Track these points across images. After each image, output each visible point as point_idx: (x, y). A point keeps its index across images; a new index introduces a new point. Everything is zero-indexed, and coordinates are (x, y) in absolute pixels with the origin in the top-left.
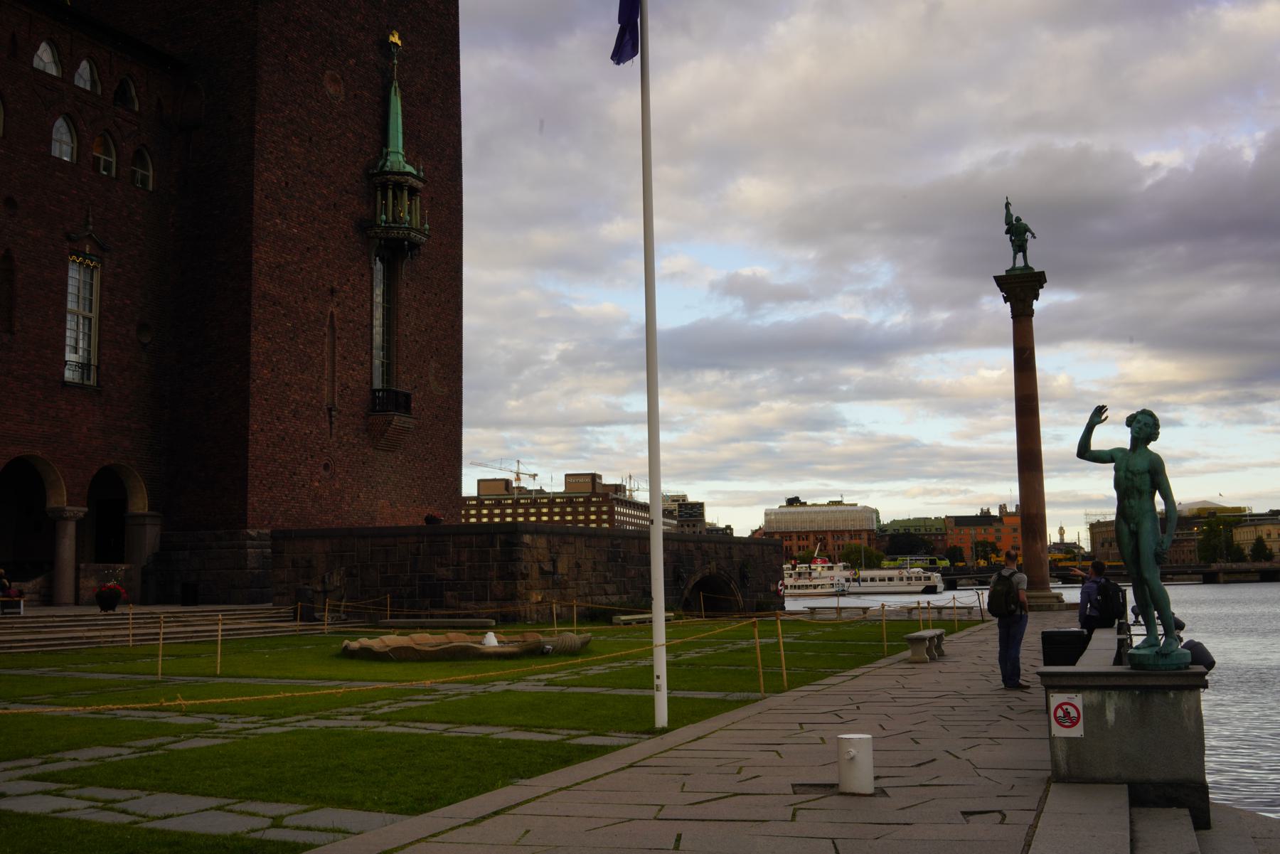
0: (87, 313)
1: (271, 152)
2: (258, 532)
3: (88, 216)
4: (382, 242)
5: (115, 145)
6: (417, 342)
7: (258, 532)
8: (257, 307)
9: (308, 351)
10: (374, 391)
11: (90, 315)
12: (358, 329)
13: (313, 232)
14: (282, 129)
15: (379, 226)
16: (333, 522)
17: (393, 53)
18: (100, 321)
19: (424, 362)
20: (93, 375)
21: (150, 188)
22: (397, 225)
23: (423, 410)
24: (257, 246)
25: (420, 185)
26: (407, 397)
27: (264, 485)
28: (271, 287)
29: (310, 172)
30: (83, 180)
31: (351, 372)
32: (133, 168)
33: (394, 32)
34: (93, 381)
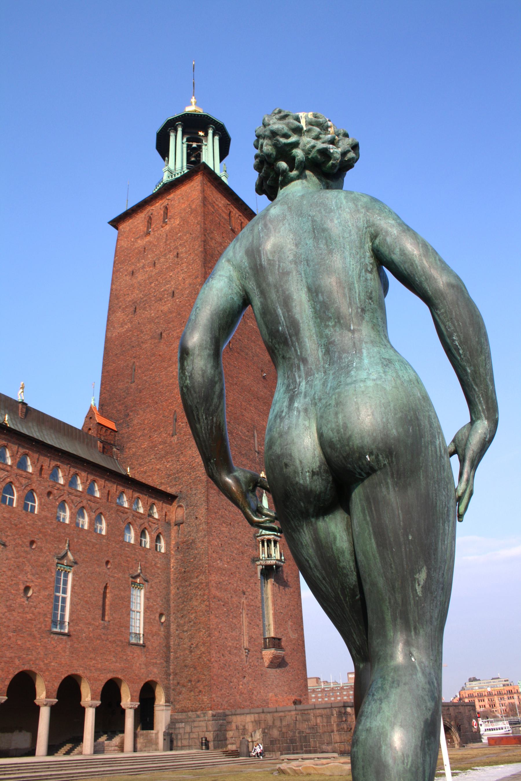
0: (138, 609)
15: (262, 560)
18: (144, 613)
20: (142, 639)
34: (141, 642)
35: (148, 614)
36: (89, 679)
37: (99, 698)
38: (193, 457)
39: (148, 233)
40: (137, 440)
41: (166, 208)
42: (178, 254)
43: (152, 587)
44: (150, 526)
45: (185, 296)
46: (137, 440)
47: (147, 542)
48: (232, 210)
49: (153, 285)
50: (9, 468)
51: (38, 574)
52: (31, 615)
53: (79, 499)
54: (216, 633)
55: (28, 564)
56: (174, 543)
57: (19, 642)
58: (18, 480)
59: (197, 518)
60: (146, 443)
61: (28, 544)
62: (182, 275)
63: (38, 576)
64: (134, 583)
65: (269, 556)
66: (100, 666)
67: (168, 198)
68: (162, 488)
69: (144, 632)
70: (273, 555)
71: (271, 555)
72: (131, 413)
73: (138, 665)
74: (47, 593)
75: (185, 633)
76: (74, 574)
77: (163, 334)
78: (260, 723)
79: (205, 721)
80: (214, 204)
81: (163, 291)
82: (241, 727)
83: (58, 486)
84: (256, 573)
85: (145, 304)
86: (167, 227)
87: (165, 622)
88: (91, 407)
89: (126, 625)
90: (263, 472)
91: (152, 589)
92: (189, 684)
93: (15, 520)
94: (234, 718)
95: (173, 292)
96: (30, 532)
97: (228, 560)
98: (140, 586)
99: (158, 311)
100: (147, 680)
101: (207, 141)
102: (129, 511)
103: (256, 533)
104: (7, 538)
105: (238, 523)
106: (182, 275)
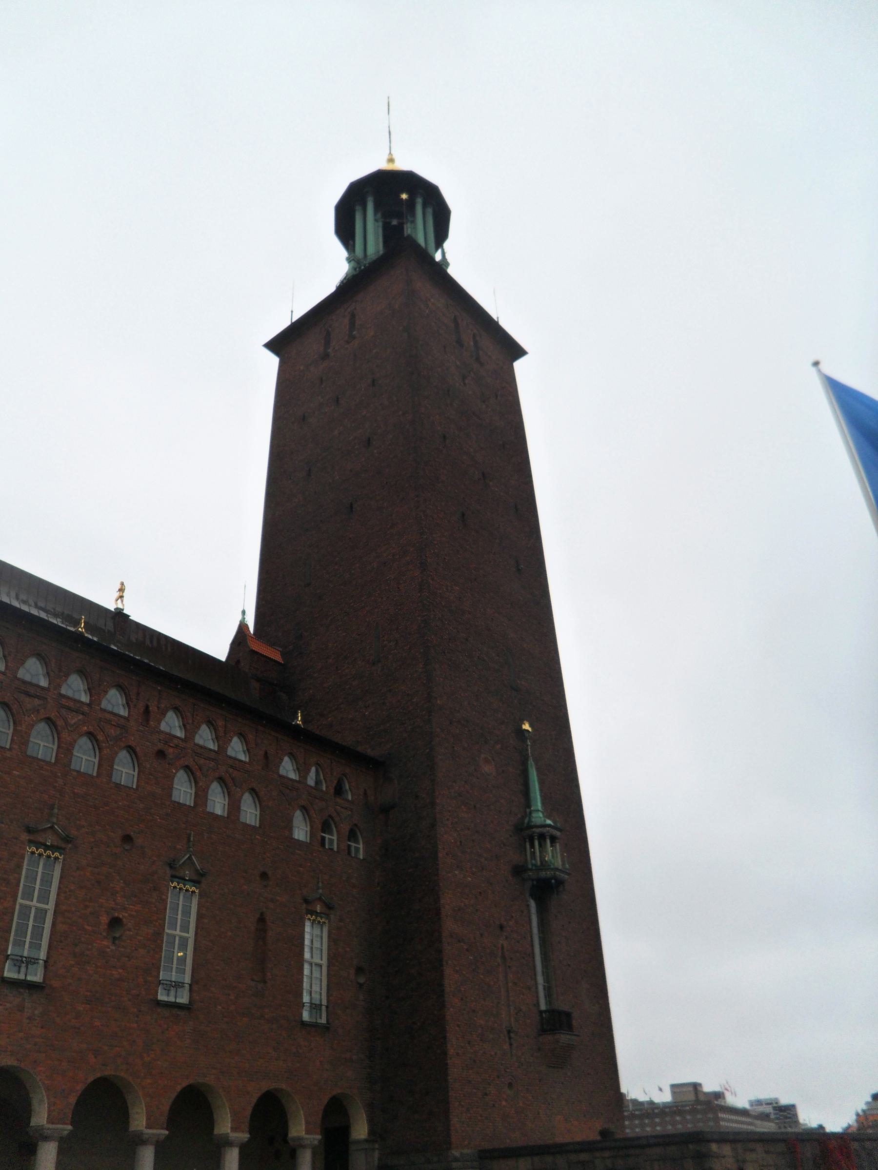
2: (461, 1153)
3: (318, 883)
4: (535, 883)
5: (336, 827)
6: (569, 965)
7: (461, 1153)
8: (447, 945)
10: (541, 1012)
12: (524, 958)
13: (483, 879)
15: (531, 870)
18: (328, 967)
21: (361, 857)
24: (443, 894)
25: (558, 834)
26: (568, 1015)
27: (463, 1106)
28: (456, 926)
30: (314, 854)
31: (522, 996)
32: (349, 843)
33: (525, 722)
34: (323, 1021)
39: (325, 356)
40: (315, 675)
41: (353, 316)
42: (373, 381)
44: (338, 814)
46: (315, 675)
47: (333, 839)
49: (336, 432)
50: (86, 708)
51: (135, 896)
52: (120, 971)
57: (97, 1023)
68: (360, 749)
69: (328, 1001)
83: (176, 741)
91: (342, 924)
95: (369, 439)
100: (334, 1093)
101: (413, 222)
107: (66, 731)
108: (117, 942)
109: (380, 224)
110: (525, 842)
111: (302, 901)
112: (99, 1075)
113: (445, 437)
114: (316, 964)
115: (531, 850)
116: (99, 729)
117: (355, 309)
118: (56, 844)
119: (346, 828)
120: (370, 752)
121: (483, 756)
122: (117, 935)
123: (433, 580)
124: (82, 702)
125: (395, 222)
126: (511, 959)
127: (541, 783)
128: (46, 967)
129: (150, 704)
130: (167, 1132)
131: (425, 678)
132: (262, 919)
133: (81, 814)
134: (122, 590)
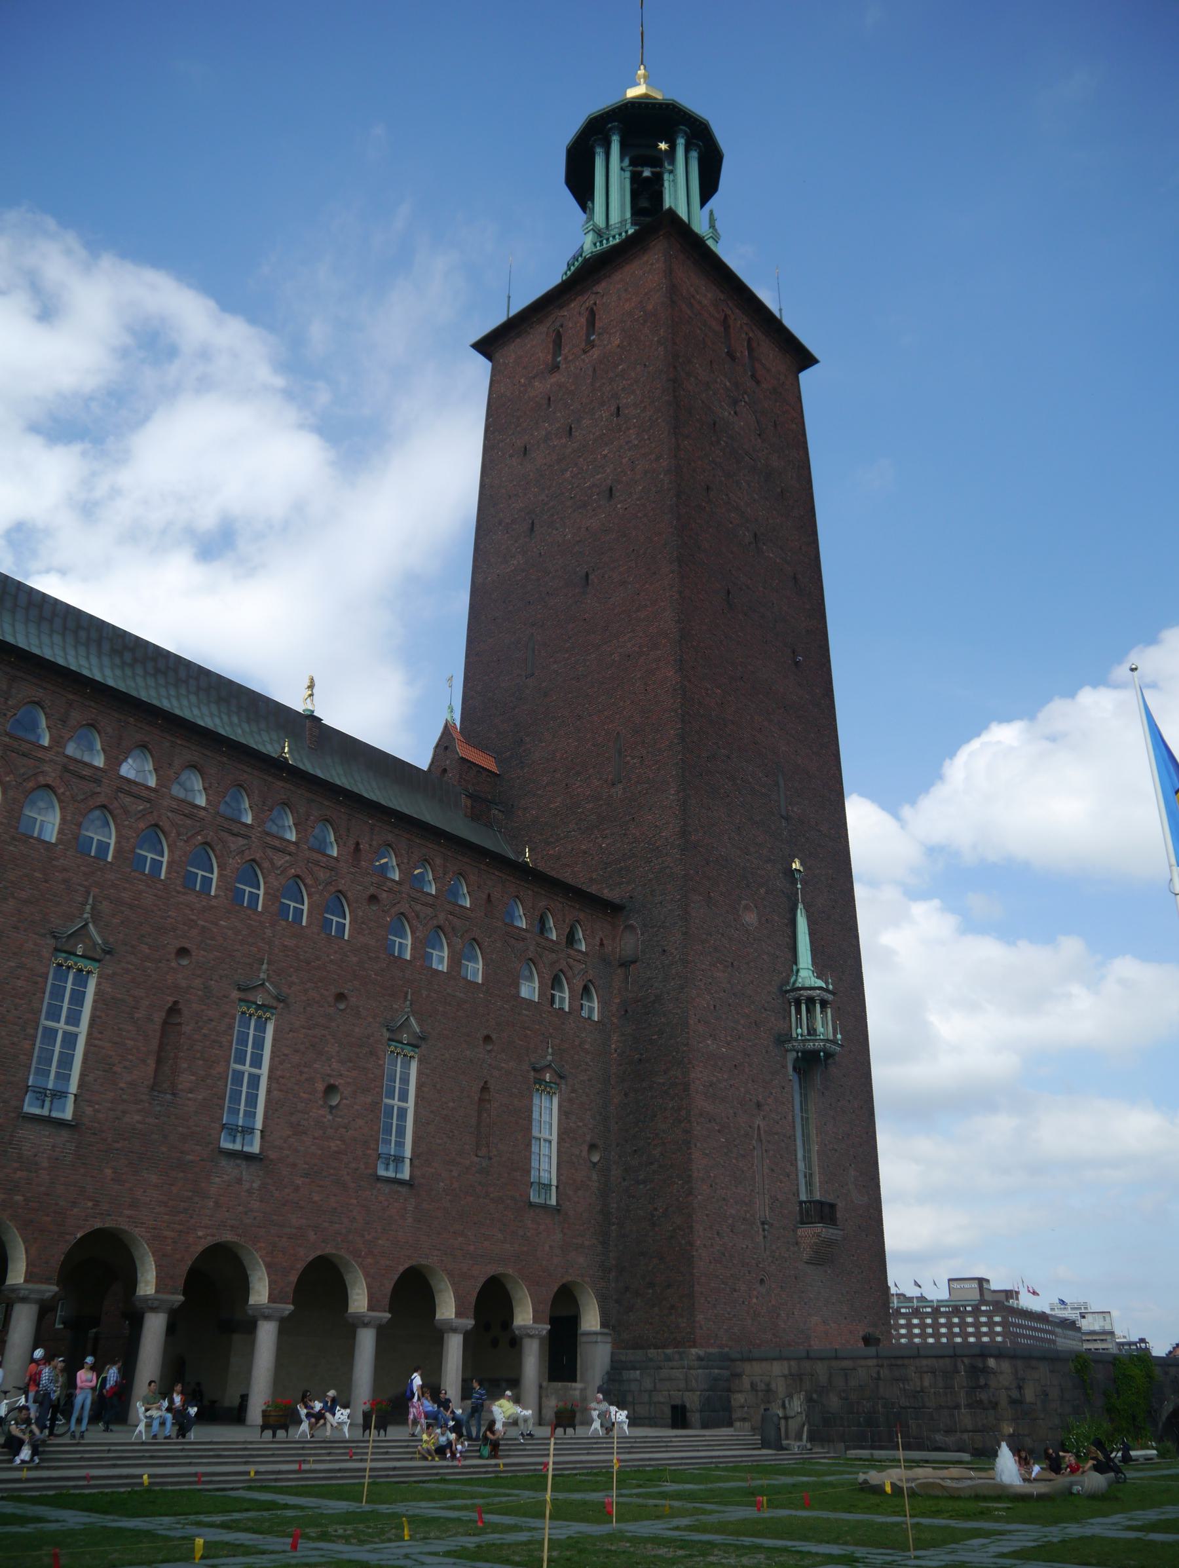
0: (547, 1136)
1: (701, 980)
4: (800, 1054)
5: (567, 983)
6: (836, 1150)
9: (741, 1165)
10: (801, 1203)
11: (550, 1138)
12: (783, 1141)
14: (709, 958)
15: (796, 1040)
16: (771, 1340)
17: (796, 879)
18: (558, 1143)
19: (844, 1171)
21: (596, 1019)
22: (812, 1037)
23: (846, 1220)
25: (830, 997)
26: (832, 1206)
29: (734, 994)
30: (544, 1015)
34: (553, 1202)
35: (567, 1145)
36: (451, 1275)
37: (471, 1313)
38: (657, 826)
39: (555, 368)
41: (592, 314)
42: (618, 409)
43: (573, 1091)
45: (635, 497)
47: (564, 998)
48: (729, 312)
49: (568, 474)
50: (292, 848)
51: (351, 1062)
52: (338, 1142)
53: (429, 911)
54: (705, 1187)
55: (333, 1041)
56: (617, 1001)
57: (316, 1198)
58: (311, 873)
59: (664, 951)
60: (559, 799)
61: (331, 999)
62: (629, 454)
63: (351, 1065)
64: (540, 1081)
65: (812, 1031)
66: (472, 1248)
67: (594, 289)
68: (593, 889)
69: (558, 1181)
70: (820, 1029)
71: (815, 1030)
72: (527, 739)
73: (547, 1248)
74: (369, 1099)
75: (641, 1187)
76: (420, 1061)
77: (591, 577)
78: (801, 1380)
79: (684, 1368)
80: (692, 300)
81: (589, 488)
82: (762, 1386)
83: (389, 884)
84: (784, 1067)
85: (552, 515)
86: (595, 353)
87: (599, 1161)
88: (446, 724)
89: (522, 1165)
90: (797, 860)
91: (574, 1095)
92: (651, 1291)
93: (306, 952)
94: (747, 1367)
95: (611, 489)
96: (336, 977)
97: (729, 1038)
98: (551, 1088)
99: (580, 528)
100: (564, 1281)
102: (528, 935)
103: (783, 985)
104: (290, 987)
105: (747, 964)
106: (629, 454)
107: (273, 874)
108: (334, 1111)
109: (628, 174)
110: (790, 1006)
111: (530, 1069)
112: (319, 1253)
113: (708, 488)
114: (545, 1140)
115: (797, 1018)
116: (307, 872)
117: (595, 304)
118: (266, 1003)
119: (579, 984)
120: (607, 894)
121: (744, 902)
122: (334, 1103)
123: (690, 681)
124: (288, 841)
125: (647, 173)
126: (769, 1142)
127: (812, 934)
128: (262, 1137)
129: (360, 841)
130: (389, 1315)
131: (677, 808)
132: (485, 1088)
133: (292, 969)
134: (311, 686)
